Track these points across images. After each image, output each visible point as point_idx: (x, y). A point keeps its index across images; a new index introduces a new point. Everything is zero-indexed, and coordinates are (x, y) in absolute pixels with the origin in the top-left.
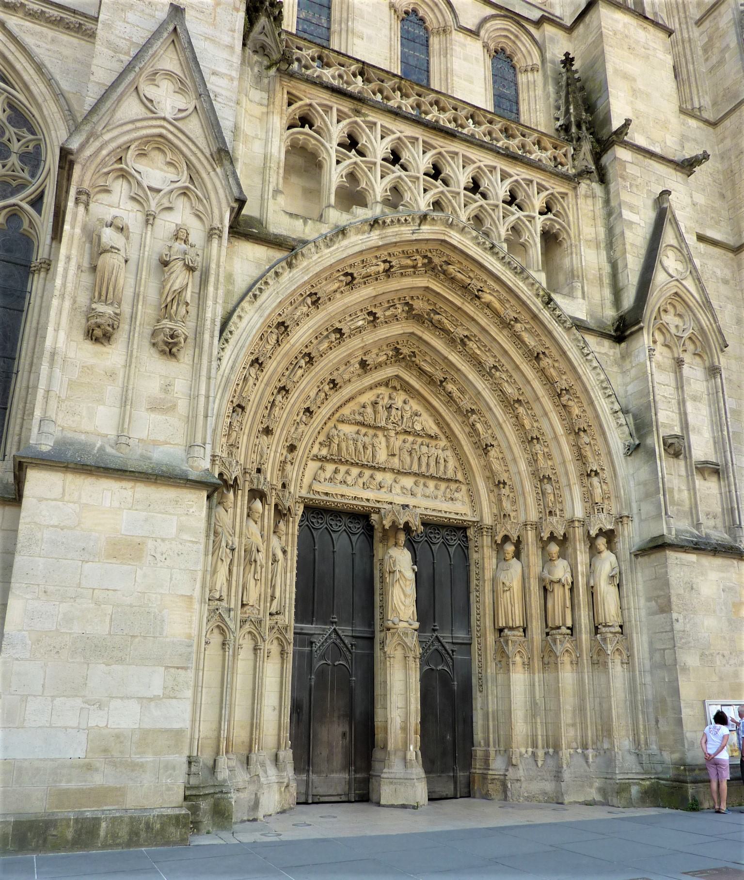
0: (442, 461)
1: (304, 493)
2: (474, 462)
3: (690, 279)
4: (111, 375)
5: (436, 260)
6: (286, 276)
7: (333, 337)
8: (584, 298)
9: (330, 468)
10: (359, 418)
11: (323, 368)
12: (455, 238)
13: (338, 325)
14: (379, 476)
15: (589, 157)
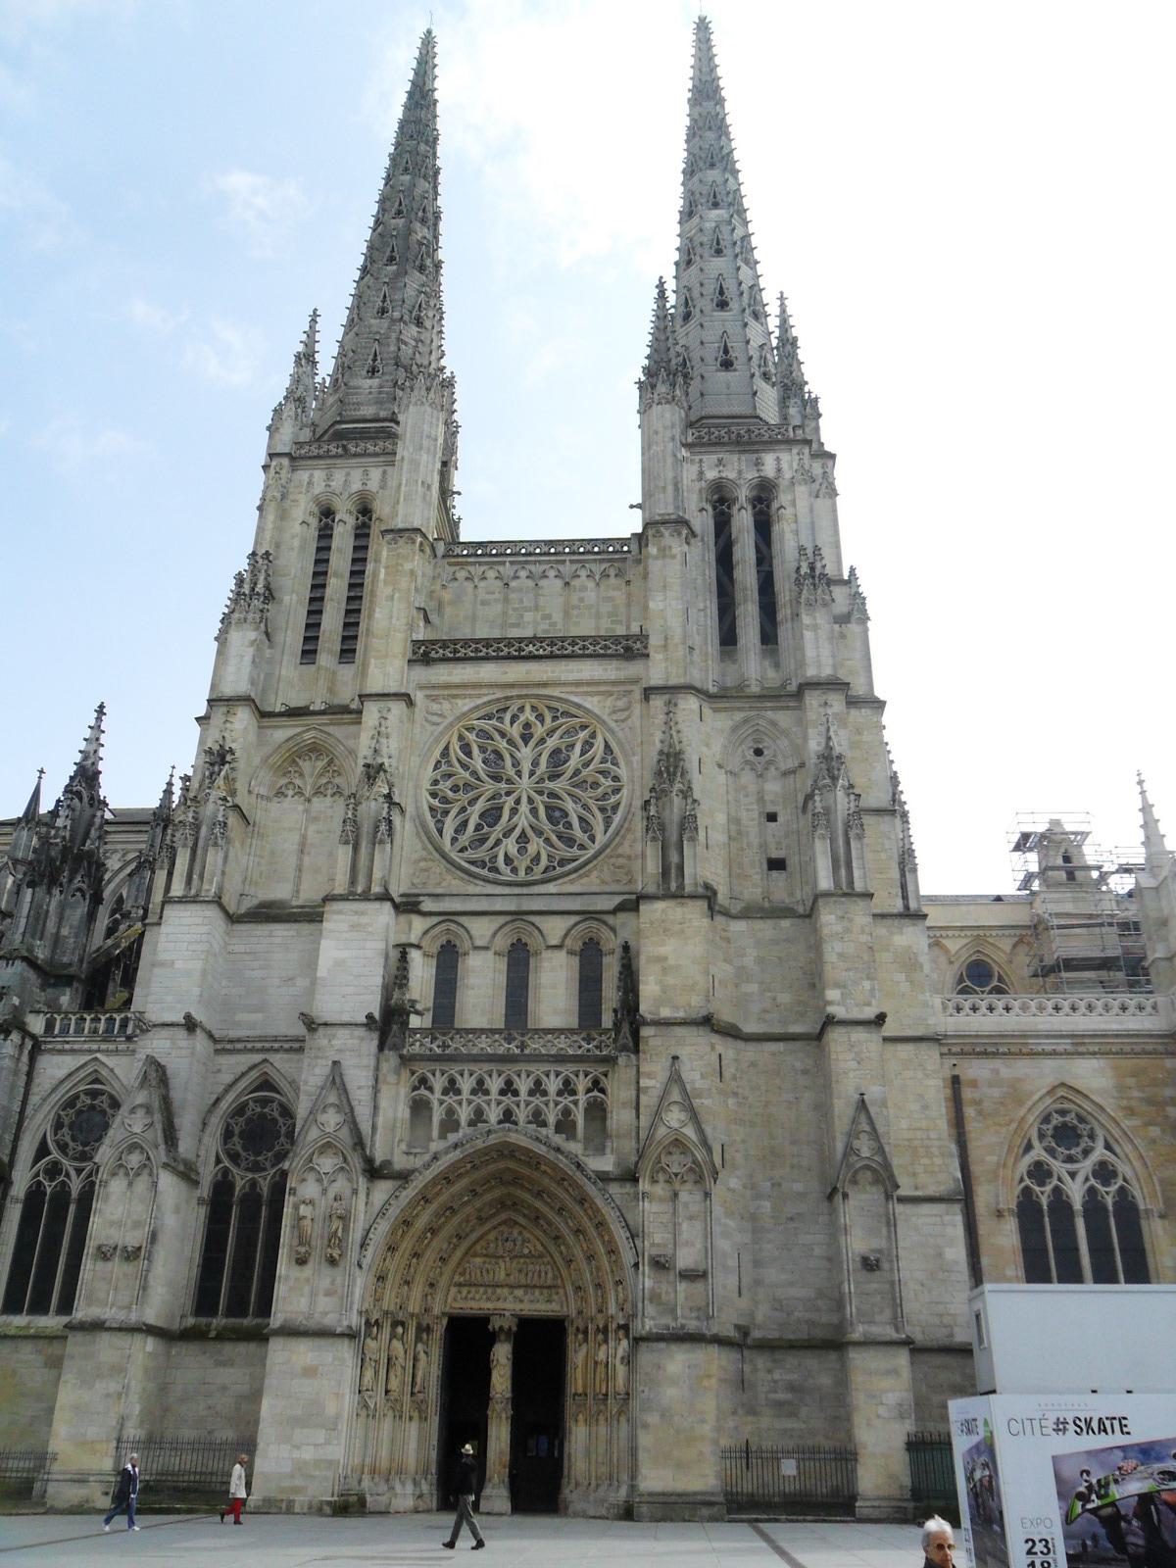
0: (543, 1274)
1: (447, 1310)
2: (565, 1272)
4: (308, 1280)
5: (506, 1152)
6: (404, 1193)
8: (612, 1153)
9: (465, 1291)
10: (484, 1252)
11: (449, 1229)
12: (514, 1138)
14: (499, 1291)
15: (628, 1035)
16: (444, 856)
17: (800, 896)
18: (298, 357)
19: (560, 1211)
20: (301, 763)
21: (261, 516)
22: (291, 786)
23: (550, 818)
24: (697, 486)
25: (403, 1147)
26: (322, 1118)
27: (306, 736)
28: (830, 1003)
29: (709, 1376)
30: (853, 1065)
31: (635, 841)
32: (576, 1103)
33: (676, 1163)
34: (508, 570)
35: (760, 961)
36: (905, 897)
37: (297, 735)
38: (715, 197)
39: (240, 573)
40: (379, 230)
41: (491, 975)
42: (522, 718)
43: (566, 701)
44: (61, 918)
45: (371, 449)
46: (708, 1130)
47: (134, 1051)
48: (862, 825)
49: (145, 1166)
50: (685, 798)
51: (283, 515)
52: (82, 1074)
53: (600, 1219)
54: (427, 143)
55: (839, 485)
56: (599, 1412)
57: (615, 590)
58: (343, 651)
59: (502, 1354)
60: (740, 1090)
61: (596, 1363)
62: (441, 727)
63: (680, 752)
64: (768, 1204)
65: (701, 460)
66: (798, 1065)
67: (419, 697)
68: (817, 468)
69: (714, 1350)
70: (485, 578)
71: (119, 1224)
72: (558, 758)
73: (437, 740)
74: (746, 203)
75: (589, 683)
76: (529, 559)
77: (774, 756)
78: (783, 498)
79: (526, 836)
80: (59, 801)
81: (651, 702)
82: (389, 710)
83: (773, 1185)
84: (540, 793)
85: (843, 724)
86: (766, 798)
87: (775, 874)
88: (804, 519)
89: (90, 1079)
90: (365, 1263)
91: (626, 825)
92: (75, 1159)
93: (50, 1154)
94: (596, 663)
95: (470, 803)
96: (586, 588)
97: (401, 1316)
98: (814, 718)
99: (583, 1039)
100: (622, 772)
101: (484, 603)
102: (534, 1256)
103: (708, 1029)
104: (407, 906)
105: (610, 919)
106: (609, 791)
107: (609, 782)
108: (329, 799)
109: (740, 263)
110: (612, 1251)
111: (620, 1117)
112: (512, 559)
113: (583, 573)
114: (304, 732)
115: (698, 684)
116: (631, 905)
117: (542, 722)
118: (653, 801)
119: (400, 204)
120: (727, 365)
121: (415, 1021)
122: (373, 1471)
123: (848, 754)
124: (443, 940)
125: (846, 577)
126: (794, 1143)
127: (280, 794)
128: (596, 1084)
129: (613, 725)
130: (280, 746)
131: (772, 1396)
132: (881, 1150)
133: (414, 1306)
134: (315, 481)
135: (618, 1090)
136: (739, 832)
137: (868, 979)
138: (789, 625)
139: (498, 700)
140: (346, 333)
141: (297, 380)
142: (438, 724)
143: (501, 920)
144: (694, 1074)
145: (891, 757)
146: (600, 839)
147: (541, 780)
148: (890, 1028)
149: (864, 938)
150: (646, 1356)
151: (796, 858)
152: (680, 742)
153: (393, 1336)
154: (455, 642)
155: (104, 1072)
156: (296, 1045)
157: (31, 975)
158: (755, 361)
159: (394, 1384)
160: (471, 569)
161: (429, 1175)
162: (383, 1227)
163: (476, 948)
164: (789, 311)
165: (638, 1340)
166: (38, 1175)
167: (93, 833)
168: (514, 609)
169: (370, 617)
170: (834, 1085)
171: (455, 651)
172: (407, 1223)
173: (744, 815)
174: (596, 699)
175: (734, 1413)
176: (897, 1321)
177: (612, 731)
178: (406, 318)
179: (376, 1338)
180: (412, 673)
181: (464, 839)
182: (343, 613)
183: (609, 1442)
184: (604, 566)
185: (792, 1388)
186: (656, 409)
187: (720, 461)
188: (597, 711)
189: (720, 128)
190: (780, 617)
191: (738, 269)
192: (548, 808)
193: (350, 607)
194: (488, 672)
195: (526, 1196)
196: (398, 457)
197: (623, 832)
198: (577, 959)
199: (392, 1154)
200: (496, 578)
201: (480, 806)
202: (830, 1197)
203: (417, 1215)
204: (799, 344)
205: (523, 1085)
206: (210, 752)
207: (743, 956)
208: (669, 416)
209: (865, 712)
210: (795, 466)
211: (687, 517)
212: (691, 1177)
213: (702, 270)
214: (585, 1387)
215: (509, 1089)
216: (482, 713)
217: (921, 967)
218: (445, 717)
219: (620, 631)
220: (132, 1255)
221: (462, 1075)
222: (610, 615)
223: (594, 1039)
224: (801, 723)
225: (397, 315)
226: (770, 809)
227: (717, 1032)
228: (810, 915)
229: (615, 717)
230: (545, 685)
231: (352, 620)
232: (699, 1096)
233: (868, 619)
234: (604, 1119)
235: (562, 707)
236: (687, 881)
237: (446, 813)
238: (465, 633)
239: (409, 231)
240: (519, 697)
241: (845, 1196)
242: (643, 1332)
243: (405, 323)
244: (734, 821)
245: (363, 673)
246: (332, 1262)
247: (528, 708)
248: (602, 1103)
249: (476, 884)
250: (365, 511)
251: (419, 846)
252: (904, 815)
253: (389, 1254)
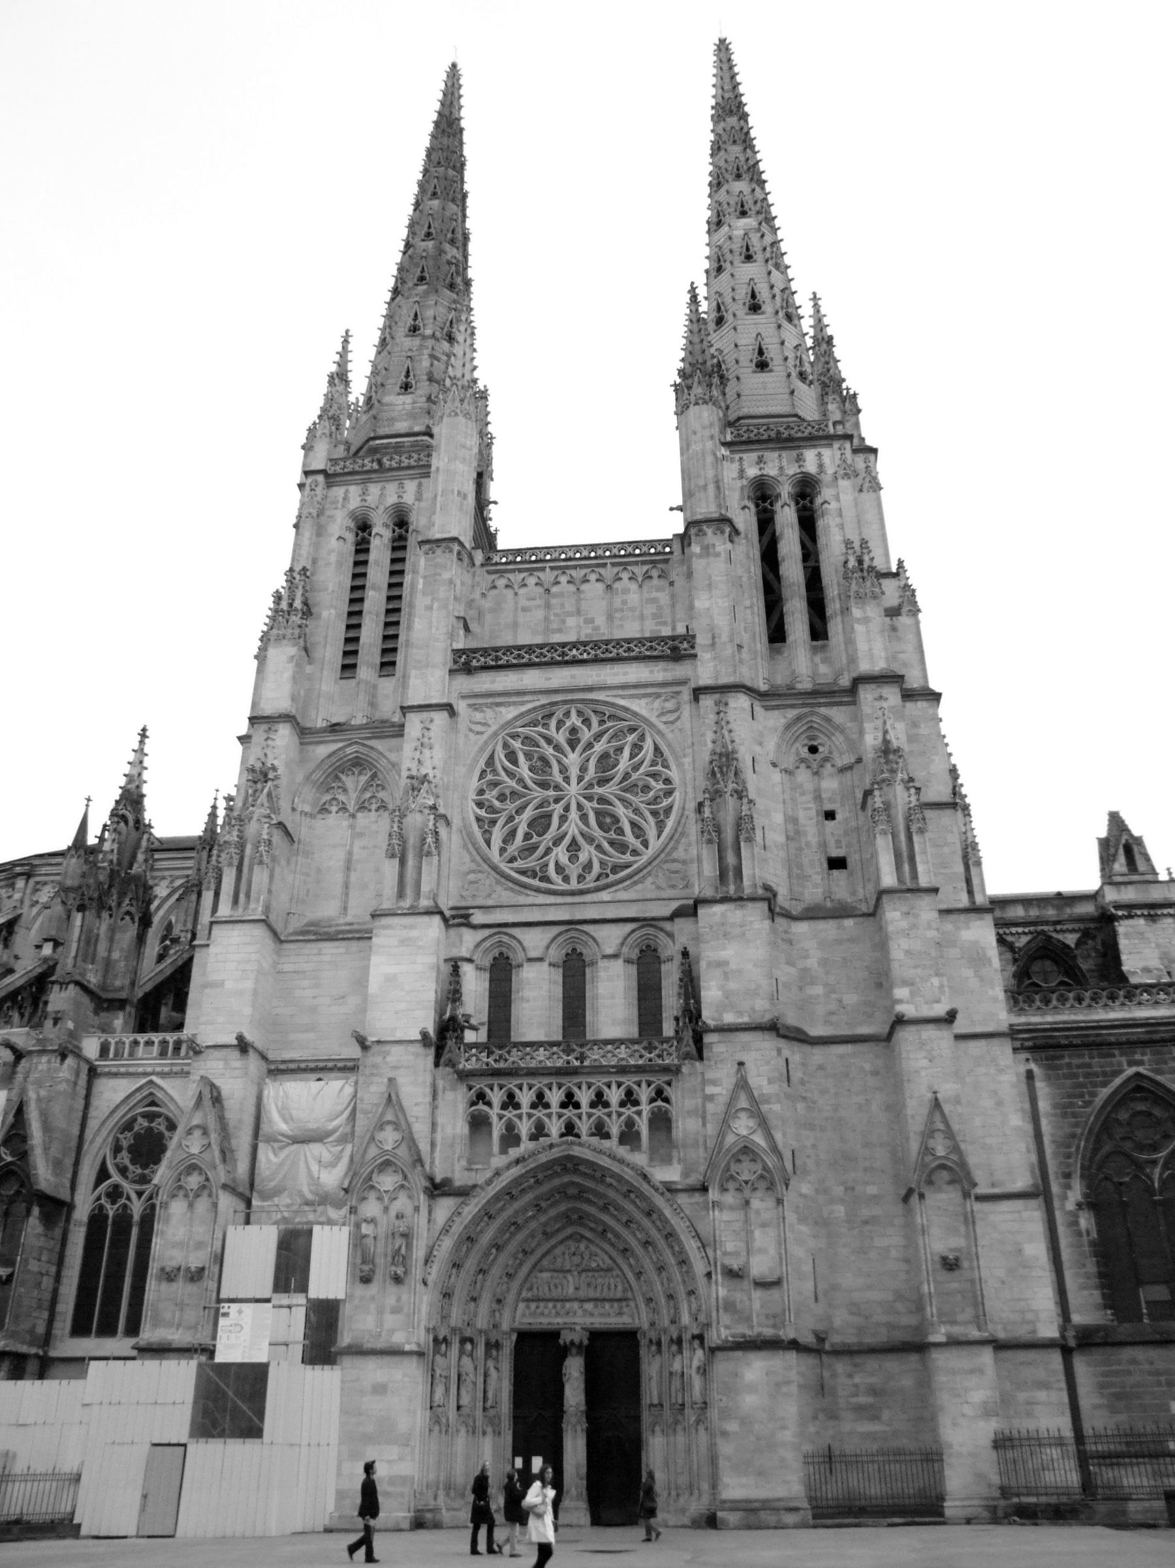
0: (613, 1287)
1: (516, 1325)
3: (759, 1132)
4: (373, 1298)
5: (569, 1165)
7: (512, 1229)
8: (679, 1161)
9: (533, 1305)
10: (552, 1267)
11: (512, 1247)
12: (577, 1151)
13: (514, 1220)
14: (568, 1305)
15: (691, 1042)
16: (495, 868)
17: (863, 894)
18: (331, 377)
19: (627, 1224)
20: (343, 777)
21: (297, 534)
22: (334, 803)
23: (601, 825)
24: (739, 484)
25: (464, 1163)
26: (380, 1136)
27: (349, 750)
28: (900, 1001)
29: (788, 1383)
30: (925, 1063)
31: (690, 844)
32: (639, 1113)
33: (746, 1171)
34: (548, 576)
35: (824, 962)
36: (970, 892)
37: (340, 749)
38: (742, 206)
39: (277, 591)
40: (410, 252)
41: (546, 987)
42: (568, 724)
43: (613, 705)
44: (111, 940)
45: (406, 462)
46: (778, 1137)
47: (188, 1073)
48: (924, 819)
49: (204, 1187)
50: (740, 798)
51: (320, 531)
52: (138, 1097)
53: (668, 1229)
54: (454, 168)
55: (882, 479)
56: (677, 1422)
58: (383, 665)
59: (574, 1369)
60: (808, 1095)
61: (671, 1373)
62: (485, 736)
63: (734, 752)
64: (842, 1208)
65: (741, 459)
66: (867, 1067)
67: (461, 706)
68: (859, 461)
69: (792, 1357)
70: (525, 585)
71: (180, 1245)
73: (482, 750)
74: (774, 211)
75: (636, 686)
76: (569, 563)
77: (830, 753)
78: (826, 493)
79: (577, 844)
80: (105, 826)
81: (701, 703)
82: (432, 721)
83: (846, 1189)
84: (589, 798)
85: (900, 716)
86: (824, 795)
87: (835, 872)
88: (849, 514)
89: (146, 1102)
90: (431, 1279)
91: (680, 829)
92: (134, 1182)
93: (108, 1177)
94: (642, 665)
95: (517, 812)
96: (629, 590)
97: (468, 1333)
98: (869, 712)
99: (645, 1048)
100: (674, 774)
101: (524, 610)
102: (602, 1270)
103: (774, 1034)
104: (458, 919)
105: (667, 926)
106: (661, 794)
107: (661, 786)
108: (373, 813)
109: (771, 268)
110: (683, 1262)
111: (685, 1126)
112: (552, 564)
113: (625, 576)
114: (346, 746)
115: (749, 683)
116: (690, 911)
117: (589, 727)
118: (707, 803)
119: (429, 227)
120: (762, 366)
121: (470, 1036)
122: (448, 1487)
123: (906, 747)
124: (496, 953)
125: (894, 570)
126: (866, 1145)
127: (324, 810)
128: (659, 1094)
129: (662, 727)
130: (322, 761)
131: (854, 1400)
132: (956, 1149)
133: (482, 1322)
134: (350, 497)
135: (682, 1100)
136: (797, 832)
137: (937, 975)
138: (839, 619)
139: (543, 706)
140: (379, 353)
141: (330, 399)
142: (482, 733)
143: (556, 930)
144: (761, 1080)
145: (949, 750)
146: (655, 844)
147: (590, 786)
148: (961, 1026)
149: (931, 934)
150: (723, 1366)
151: (857, 857)
152: (733, 742)
153: (462, 1352)
154: (496, 649)
155: (160, 1095)
156: (350, 1064)
157: (86, 1000)
158: (791, 362)
159: (465, 1400)
160: (511, 576)
161: (492, 1191)
162: (447, 1243)
163: (530, 960)
164: (823, 311)
165: (713, 1350)
166: (99, 1198)
167: (140, 857)
168: (556, 615)
169: (409, 628)
170: (906, 1084)
171: (497, 658)
172: (470, 1239)
173: (801, 815)
174: (643, 701)
175: (815, 1418)
176: (980, 1319)
177: (659, 732)
178: (438, 334)
179: (445, 1355)
180: (454, 683)
181: (512, 849)
182: (382, 624)
183: (688, 1450)
184: (646, 568)
185: (873, 1391)
186: (693, 411)
187: (760, 460)
188: (644, 712)
189: (744, 141)
190: (829, 611)
191: (769, 273)
192: (598, 813)
193: (389, 620)
194: (532, 679)
195: (592, 1210)
196: (433, 469)
197: (676, 836)
198: (635, 967)
199: (453, 1171)
200: (537, 584)
201: (528, 814)
202: (906, 1199)
203: (481, 1232)
204: (835, 342)
205: (584, 1097)
206: (252, 770)
207: (806, 957)
208: (706, 416)
209: (922, 705)
210: (838, 462)
211: (729, 515)
212: (762, 1185)
213: (732, 275)
214: (660, 1397)
215: (570, 1101)
216: (527, 719)
217: (989, 960)
218: (489, 726)
219: (666, 631)
220: (196, 1276)
221: (521, 1089)
222: (655, 616)
223: (656, 1048)
224: (858, 719)
225: (428, 332)
226: (828, 807)
227: (784, 1037)
228: (874, 913)
229: (664, 719)
230: (591, 689)
231: (391, 633)
232: (767, 1102)
233: (919, 610)
234: (669, 1129)
235: (608, 711)
236: (746, 882)
237: (493, 822)
238: (506, 639)
239: (441, 252)
240: (565, 702)
241: (922, 1196)
242: (719, 1342)
243: (437, 340)
244: (792, 820)
245: (404, 684)
246: (397, 1280)
247: (574, 713)
248: (667, 1112)
249: (527, 895)
250: (401, 522)
251: (467, 859)
252: (966, 808)
253: (454, 1271)
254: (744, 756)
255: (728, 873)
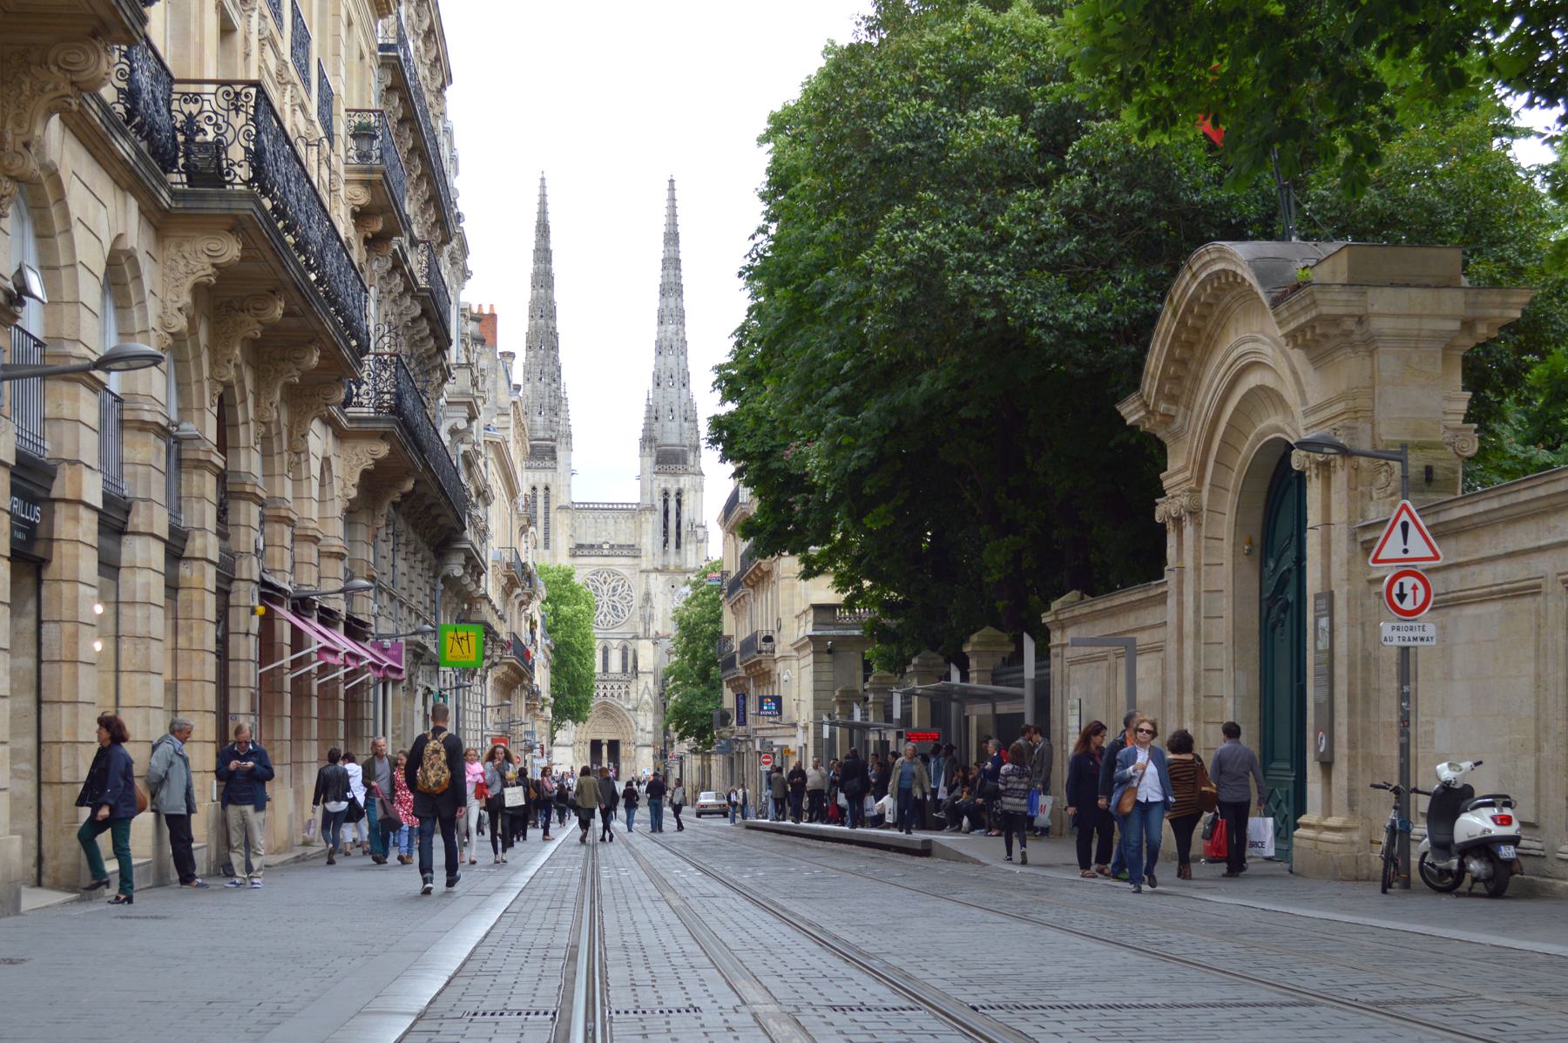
57: (630, 524)
59: (605, 748)
72: (614, 589)
78: (684, 498)
111: (633, 695)
116: (636, 637)
135: (632, 689)
150: (639, 749)
208: (650, 461)
215: (605, 688)
254: (653, 592)
255: (646, 630)
